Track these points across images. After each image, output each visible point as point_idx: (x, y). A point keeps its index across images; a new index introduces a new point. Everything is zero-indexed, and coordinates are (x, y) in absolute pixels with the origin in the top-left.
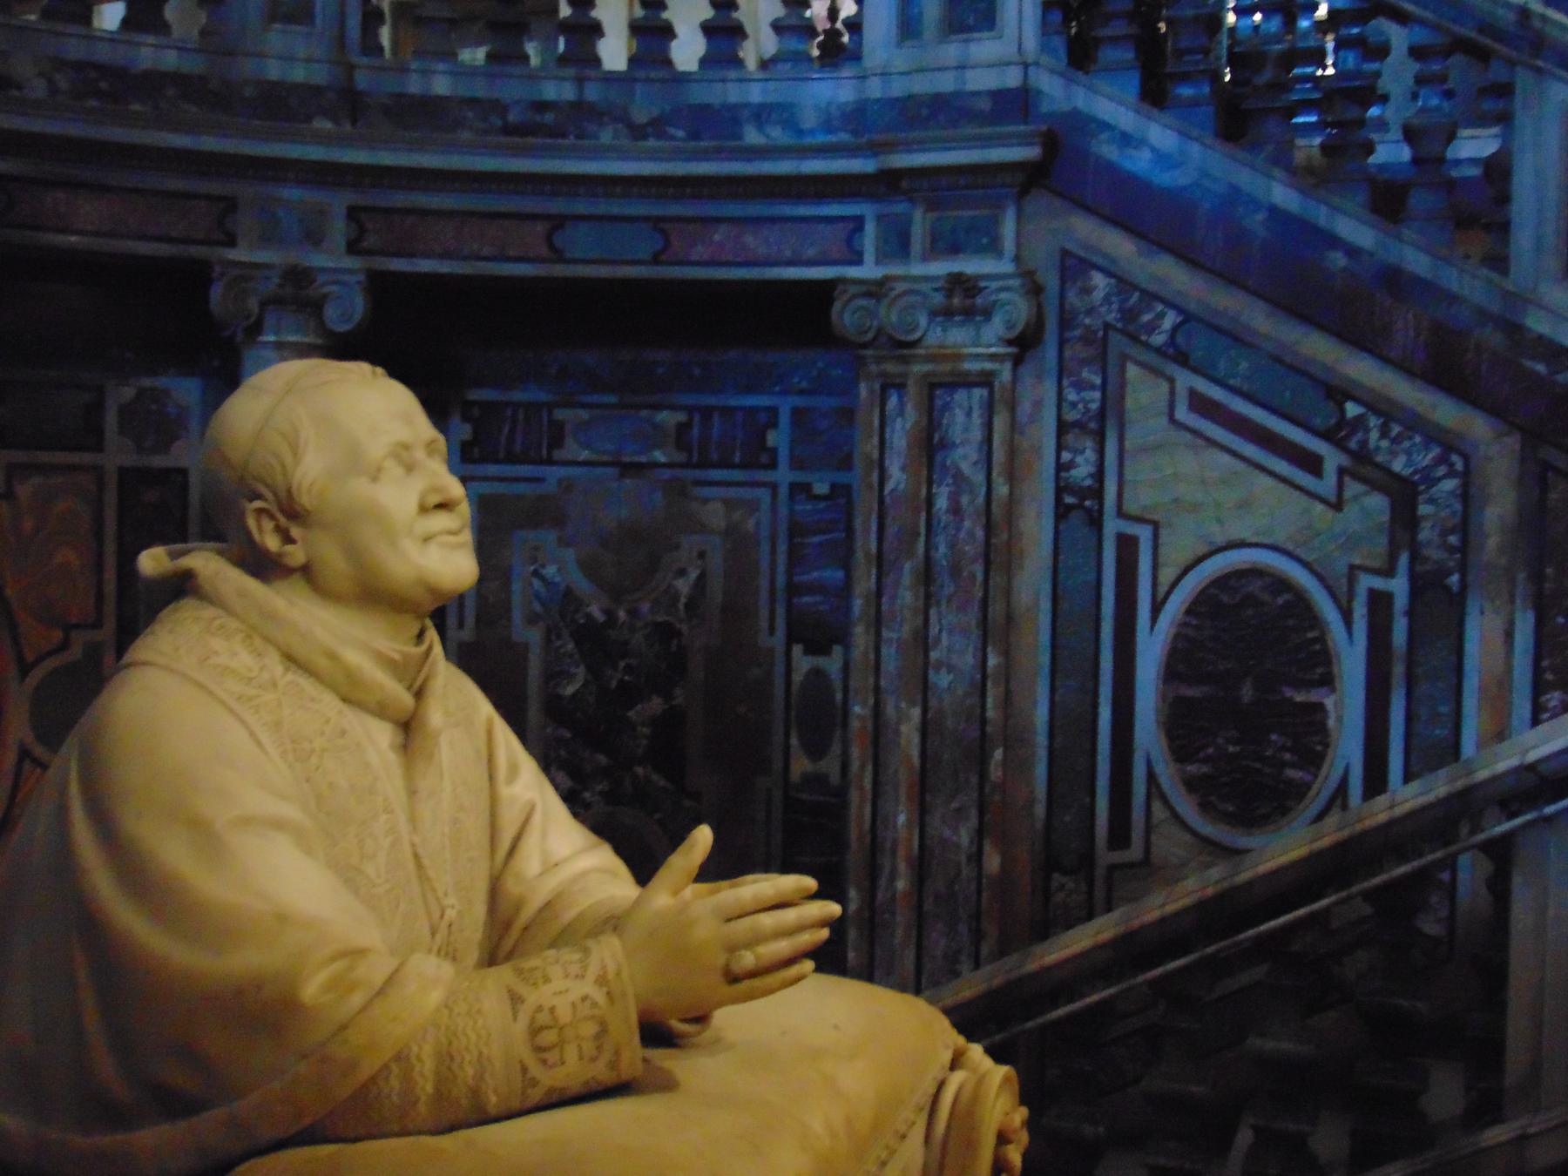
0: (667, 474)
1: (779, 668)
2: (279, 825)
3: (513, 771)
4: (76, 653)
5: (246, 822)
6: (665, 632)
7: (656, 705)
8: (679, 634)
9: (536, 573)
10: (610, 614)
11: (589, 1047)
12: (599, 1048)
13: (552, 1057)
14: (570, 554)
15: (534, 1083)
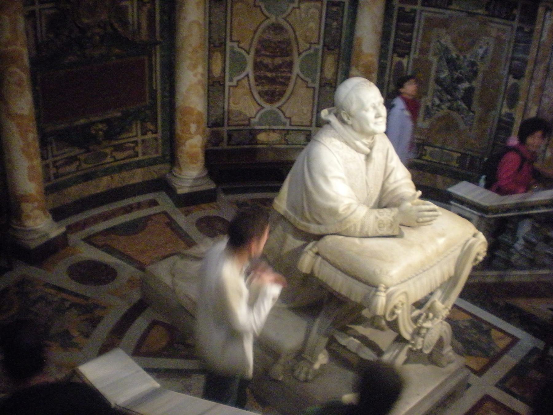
0: (480, 17)
1: (505, 81)
2: (340, 178)
3: (392, 159)
4: (312, 51)
6: (473, 64)
7: (466, 85)
8: (477, 65)
9: (438, 41)
10: (458, 58)
13: (382, 229)
14: (449, 37)
15: (377, 232)
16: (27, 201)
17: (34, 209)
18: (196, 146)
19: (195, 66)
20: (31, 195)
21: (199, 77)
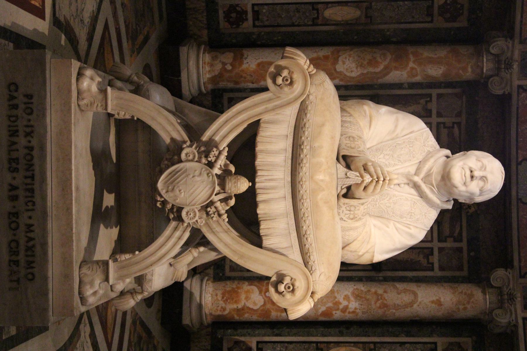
2: (396, 127)
5: (397, 120)
11: (349, 145)
12: (348, 147)
13: (348, 139)
16: (235, 59)
17: (224, 64)
18: (247, 298)
19: (358, 296)
20: (241, 63)
21: (345, 303)
